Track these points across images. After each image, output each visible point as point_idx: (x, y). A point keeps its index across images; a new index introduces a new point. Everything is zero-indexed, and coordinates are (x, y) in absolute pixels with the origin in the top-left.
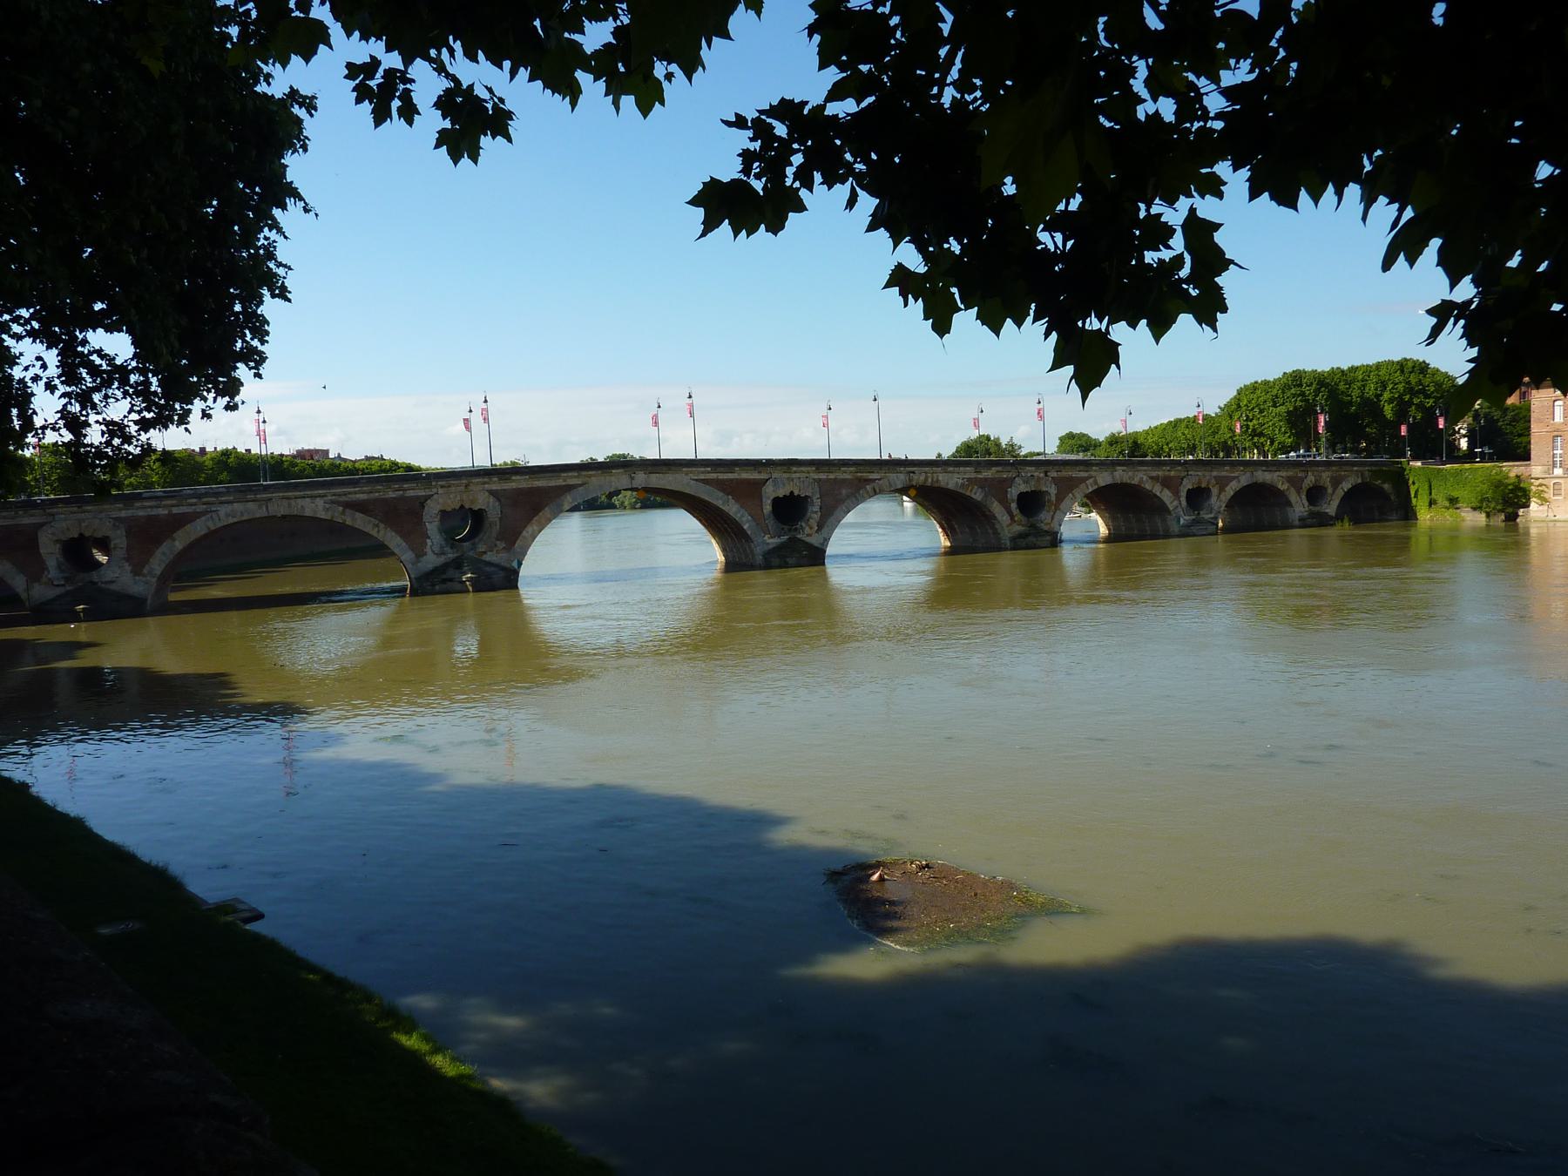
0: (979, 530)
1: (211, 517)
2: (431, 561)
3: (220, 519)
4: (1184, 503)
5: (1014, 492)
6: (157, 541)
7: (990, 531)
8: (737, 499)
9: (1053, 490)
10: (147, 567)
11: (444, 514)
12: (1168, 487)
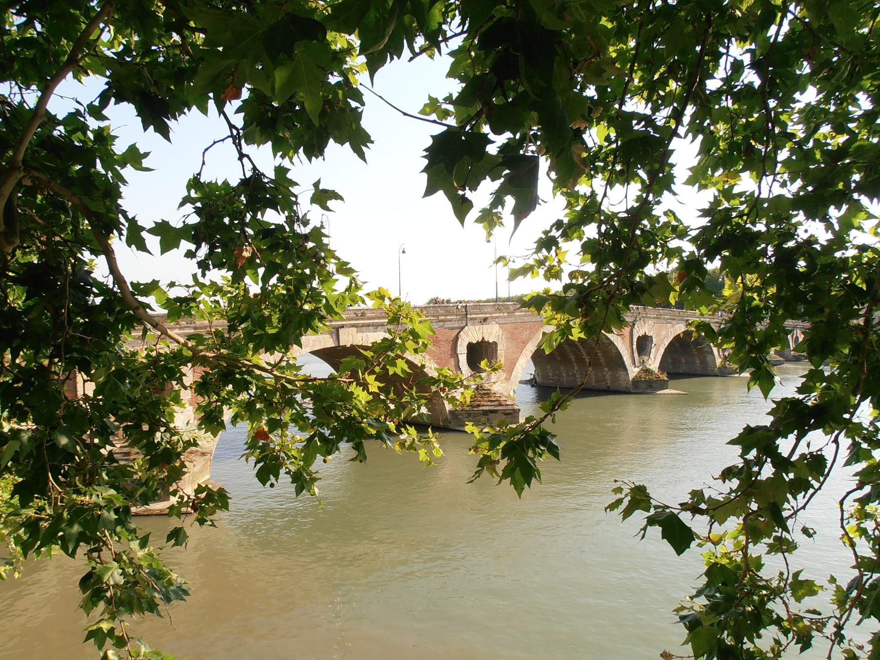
0: (683, 361)
7: (698, 362)
11: (471, 347)
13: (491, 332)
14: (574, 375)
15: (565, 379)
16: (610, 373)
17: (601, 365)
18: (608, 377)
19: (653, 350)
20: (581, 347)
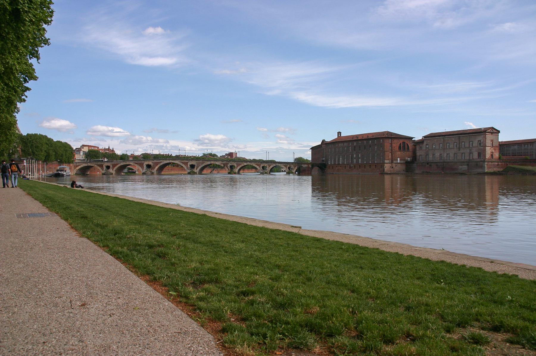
2: (144, 171)
4: (261, 168)
5: (229, 166)
6: (115, 167)
8: (184, 164)
9: (236, 165)
12: (258, 166)
13: (150, 163)
19: (196, 168)
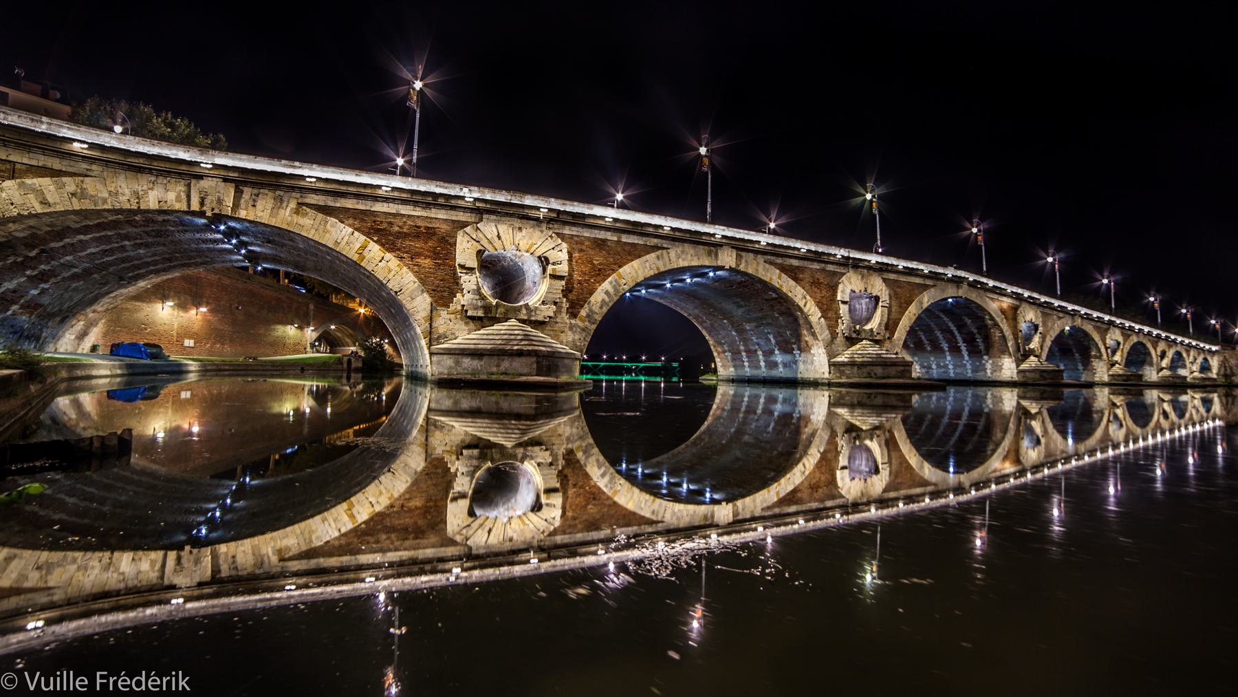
1: (662, 254)
3: (670, 260)
10: (586, 305)
14: (946, 366)
15: (935, 371)
16: (990, 362)
17: (980, 352)
18: (988, 366)
20: (956, 333)
